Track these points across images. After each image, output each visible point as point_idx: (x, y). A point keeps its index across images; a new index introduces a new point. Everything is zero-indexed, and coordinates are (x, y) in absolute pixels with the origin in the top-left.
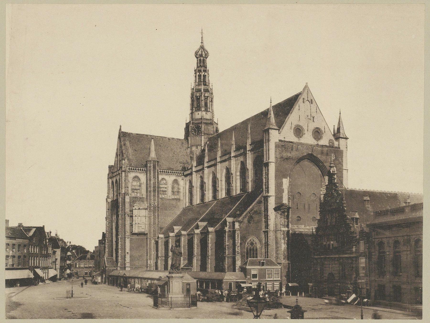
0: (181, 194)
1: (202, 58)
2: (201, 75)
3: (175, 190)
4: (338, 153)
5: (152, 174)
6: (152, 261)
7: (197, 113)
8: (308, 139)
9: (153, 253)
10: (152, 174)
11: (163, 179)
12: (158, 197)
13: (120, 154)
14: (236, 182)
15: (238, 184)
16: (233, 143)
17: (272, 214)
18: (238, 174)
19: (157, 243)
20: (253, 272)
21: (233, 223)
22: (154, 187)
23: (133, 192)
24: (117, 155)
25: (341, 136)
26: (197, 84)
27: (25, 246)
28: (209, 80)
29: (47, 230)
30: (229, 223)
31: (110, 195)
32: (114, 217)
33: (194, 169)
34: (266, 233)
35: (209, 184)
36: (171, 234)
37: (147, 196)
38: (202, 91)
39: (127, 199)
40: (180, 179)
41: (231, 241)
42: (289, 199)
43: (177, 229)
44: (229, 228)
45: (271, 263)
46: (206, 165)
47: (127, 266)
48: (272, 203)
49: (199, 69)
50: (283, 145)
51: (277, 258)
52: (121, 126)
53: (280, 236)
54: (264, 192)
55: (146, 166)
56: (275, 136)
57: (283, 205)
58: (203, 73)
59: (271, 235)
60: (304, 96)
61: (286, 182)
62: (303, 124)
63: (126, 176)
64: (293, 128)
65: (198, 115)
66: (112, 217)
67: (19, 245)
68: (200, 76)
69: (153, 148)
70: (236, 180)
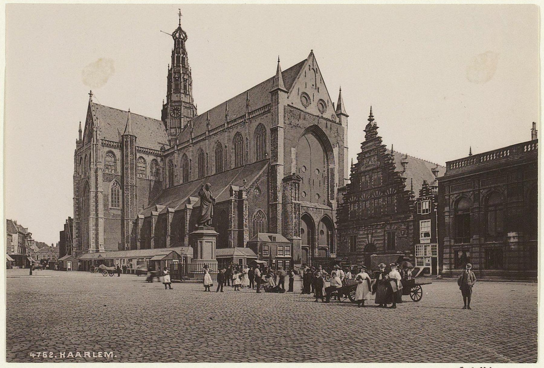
8: (313, 109)
38: (181, 72)
56: (284, 100)
58: (182, 55)
60: (310, 62)
68: (178, 58)
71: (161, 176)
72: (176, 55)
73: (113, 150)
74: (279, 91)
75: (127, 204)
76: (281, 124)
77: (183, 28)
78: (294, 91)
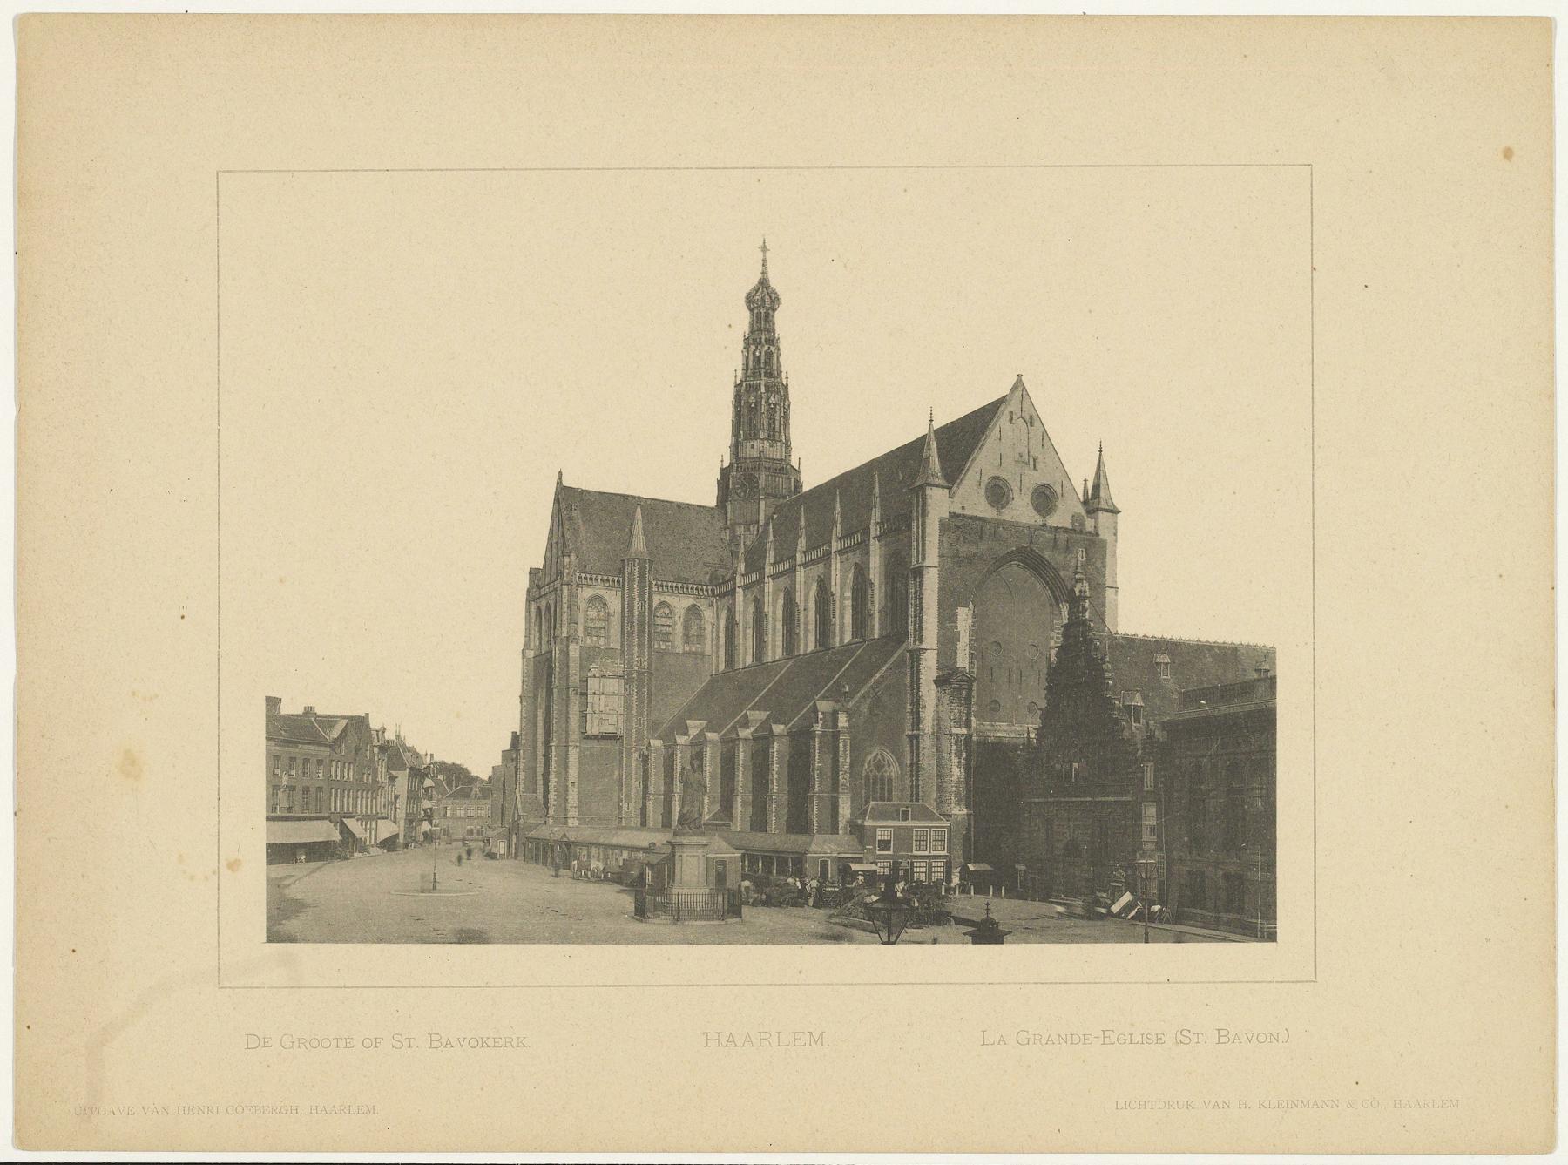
0: (708, 641)
3: (694, 631)
4: (1095, 548)
6: (632, 805)
8: (1021, 511)
9: (637, 785)
11: (662, 604)
12: (650, 647)
13: (559, 542)
14: (842, 617)
15: (848, 620)
16: (838, 518)
17: (929, 693)
18: (848, 594)
19: (645, 759)
20: (881, 836)
21: (835, 714)
22: (641, 624)
25: (1103, 505)
27: (320, 762)
28: (779, 366)
29: (374, 724)
32: (543, 694)
33: (739, 581)
34: (915, 739)
35: (775, 620)
36: (681, 740)
37: (622, 646)
39: (574, 651)
40: (703, 605)
41: (828, 757)
42: (972, 656)
43: (695, 726)
45: (925, 814)
46: (769, 570)
47: (570, 814)
48: (930, 666)
49: (757, 335)
50: (956, 525)
51: (940, 802)
53: (949, 747)
54: (912, 639)
55: (621, 572)
56: (939, 504)
57: (956, 671)
59: (927, 743)
60: (1013, 406)
61: (964, 618)
62: (1009, 474)
63: (572, 595)
65: (751, 450)
66: (535, 697)
67: (306, 761)
69: (639, 527)
70: (843, 608)
77: (773, 283)
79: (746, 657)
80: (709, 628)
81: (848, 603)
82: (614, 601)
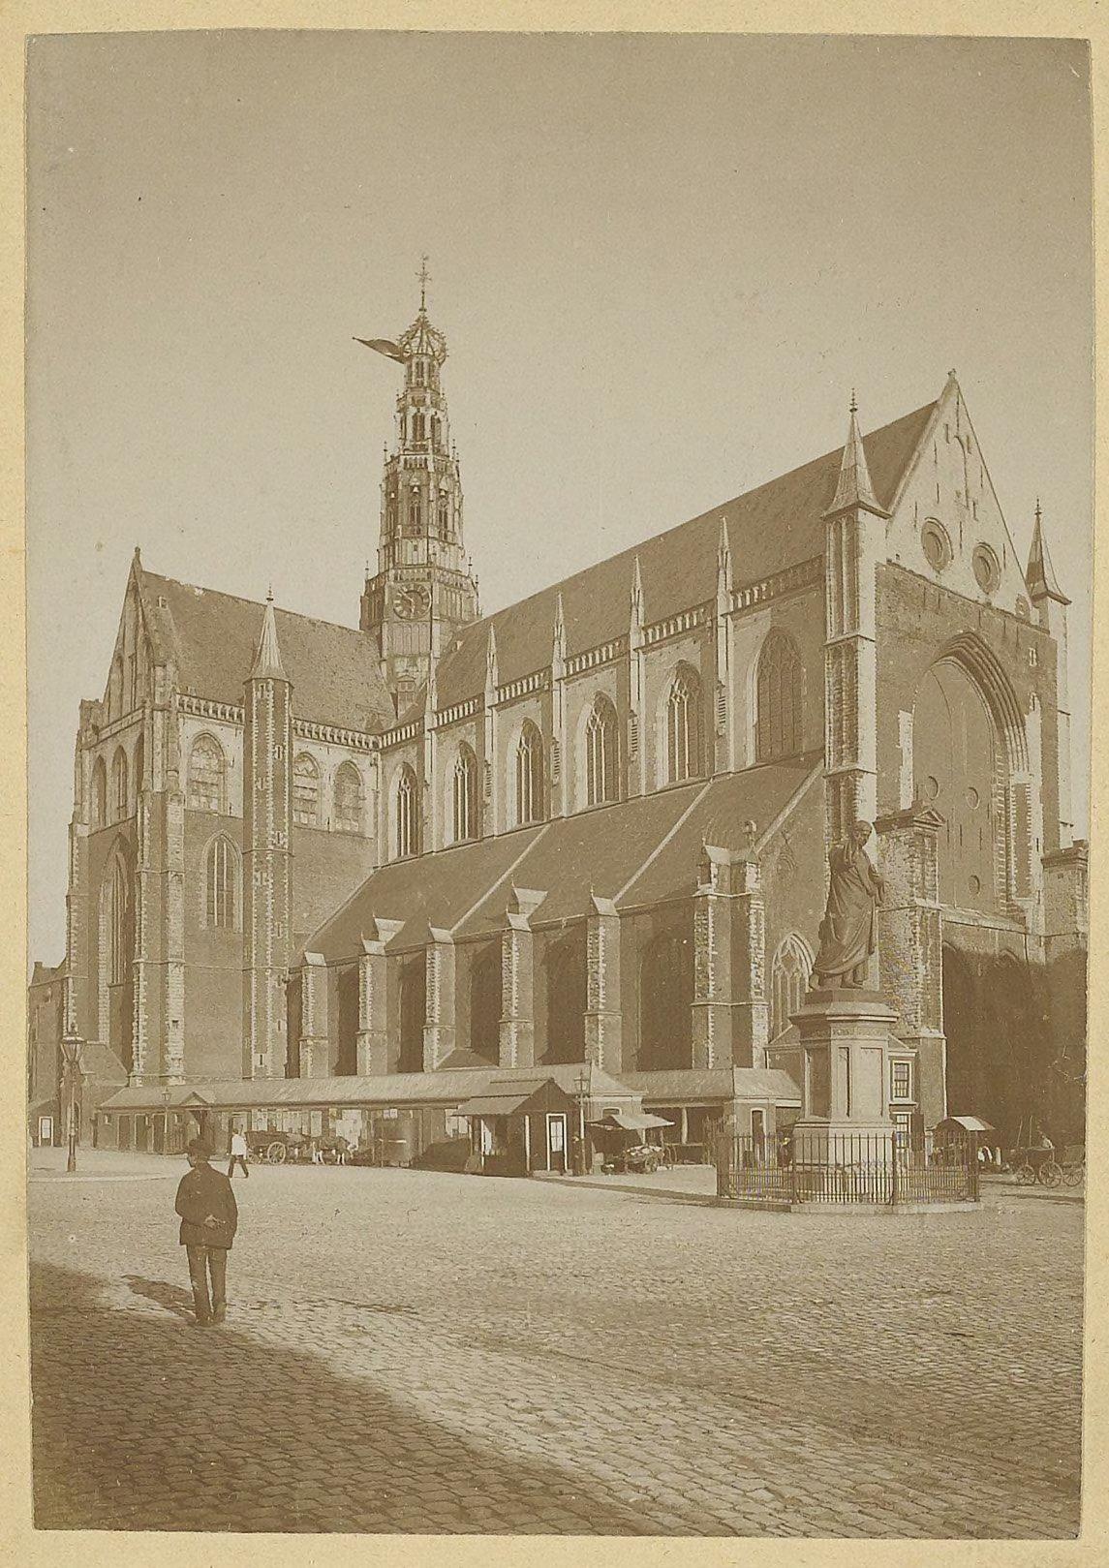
0: (370, 818)
1: (426, 360)
2: (423, 418)
3: (347, 800)
5: (271, 729)
7: (410, 545)
8: (960, 578)
9: (277, 1027)
10: (271, 729)
14: (651, 748)
18: (663, 713)
19: (294, 989)
21: (737, 868)
23: (195, 792)
24: (119, 659)
26: (408, 444)
30: (719, 866)
31: (86, 812)
32: (108, 892)
33: (430, 721)
37: (247, 812)
38: (431, 469)
39: (175, 815)
40: (363, 762)
44: (720, 888)
46: (490, 699)
47: (171, 1071)
49: (418, 394)
50: (896, 582)
52: (137, 550)
54: (831, 758)
55: (245, 701)
58: (432, 411)
60: (947, 415)
63: (171, 728)
64: (920, 524)
66: (94, 896)
68: (419, 420)
70: (652, 735)
71: (370, 818)
72: (413, 410)
73: (216, 729)
74: (861, 512)
75: (261, 916)
76: (867, 628)
77: (433, 324)
78: (904, 514)
79: (442, 830)
80: (370, 796)
81: (663, 727)
82: (232, 742)
